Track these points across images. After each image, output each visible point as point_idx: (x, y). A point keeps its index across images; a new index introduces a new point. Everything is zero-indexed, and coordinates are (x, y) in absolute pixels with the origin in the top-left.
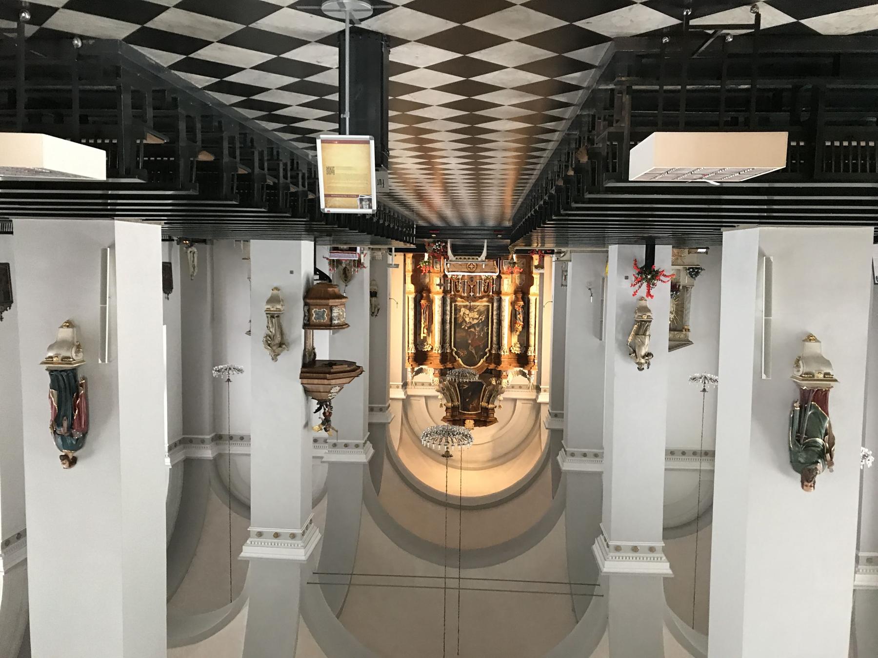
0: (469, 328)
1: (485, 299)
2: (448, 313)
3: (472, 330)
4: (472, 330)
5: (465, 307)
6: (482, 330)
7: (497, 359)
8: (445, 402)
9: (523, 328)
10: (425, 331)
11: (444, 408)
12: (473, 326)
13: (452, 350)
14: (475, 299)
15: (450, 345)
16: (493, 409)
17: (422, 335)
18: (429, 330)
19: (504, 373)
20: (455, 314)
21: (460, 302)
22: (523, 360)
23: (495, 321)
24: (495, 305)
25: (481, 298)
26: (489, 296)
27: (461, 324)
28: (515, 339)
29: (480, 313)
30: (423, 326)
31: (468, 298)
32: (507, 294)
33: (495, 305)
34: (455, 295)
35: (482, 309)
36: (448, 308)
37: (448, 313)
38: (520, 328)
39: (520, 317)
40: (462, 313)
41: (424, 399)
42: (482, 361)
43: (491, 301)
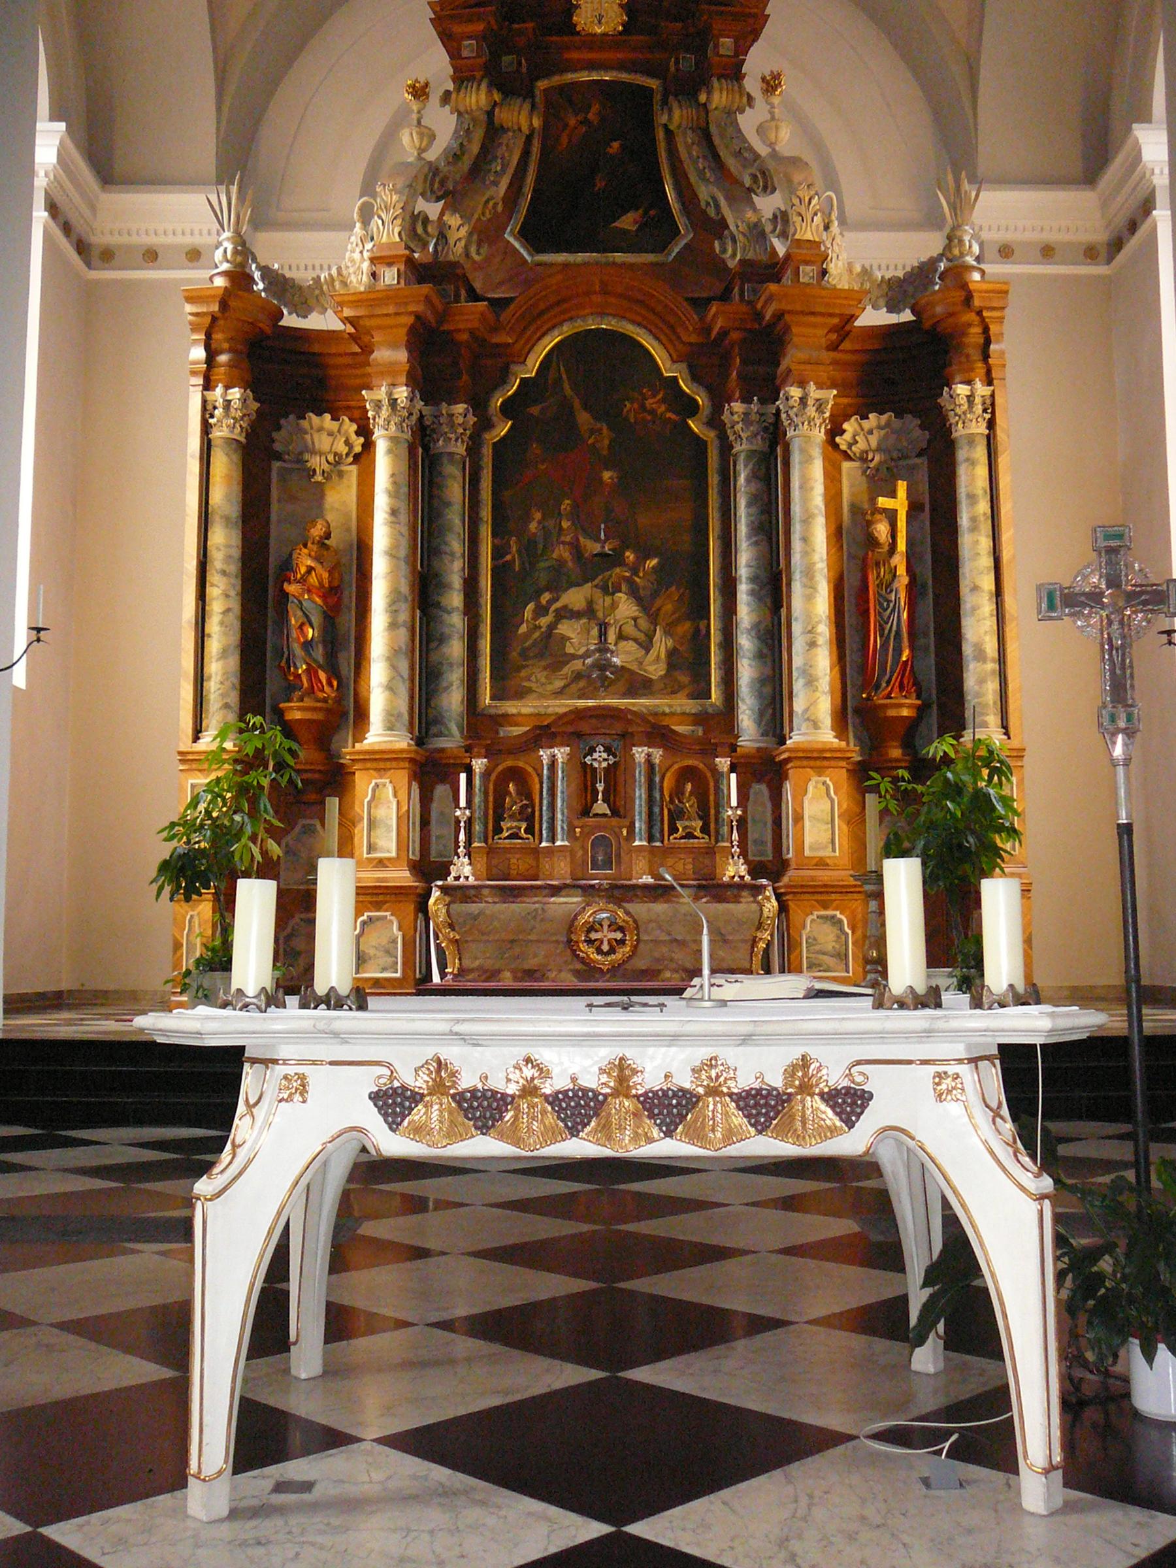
0: (612, 560)
1: (517, 731)
2: (745, 642)
3: (592, 547)
5: (637, 685)
7: (442, 363)
8: (748, 122)
9: (287, 566)
10: (882, 530)
11: (752, 84)
13: (715, 421)
14: (572, 729)
16: (462, 78)
17: (899, 503)
18: (855, 542)
19: (390, 276)
20: (700, 642)
21: (675, 706)
22: (278, 368)
23: (455, 599)
24: (453, 700)
28: (340, 499)
29: (550, 650)
30: (899, 562)
31: (623, 729)
32: (380, 760)
33: (453, 700)
35: (535, 675)
36: (746, 672)
37: (745, 642)
38: (304, 561)
39: (304, 628)
40: (662, 644)
41: (856, 200)
43: (481, 726)
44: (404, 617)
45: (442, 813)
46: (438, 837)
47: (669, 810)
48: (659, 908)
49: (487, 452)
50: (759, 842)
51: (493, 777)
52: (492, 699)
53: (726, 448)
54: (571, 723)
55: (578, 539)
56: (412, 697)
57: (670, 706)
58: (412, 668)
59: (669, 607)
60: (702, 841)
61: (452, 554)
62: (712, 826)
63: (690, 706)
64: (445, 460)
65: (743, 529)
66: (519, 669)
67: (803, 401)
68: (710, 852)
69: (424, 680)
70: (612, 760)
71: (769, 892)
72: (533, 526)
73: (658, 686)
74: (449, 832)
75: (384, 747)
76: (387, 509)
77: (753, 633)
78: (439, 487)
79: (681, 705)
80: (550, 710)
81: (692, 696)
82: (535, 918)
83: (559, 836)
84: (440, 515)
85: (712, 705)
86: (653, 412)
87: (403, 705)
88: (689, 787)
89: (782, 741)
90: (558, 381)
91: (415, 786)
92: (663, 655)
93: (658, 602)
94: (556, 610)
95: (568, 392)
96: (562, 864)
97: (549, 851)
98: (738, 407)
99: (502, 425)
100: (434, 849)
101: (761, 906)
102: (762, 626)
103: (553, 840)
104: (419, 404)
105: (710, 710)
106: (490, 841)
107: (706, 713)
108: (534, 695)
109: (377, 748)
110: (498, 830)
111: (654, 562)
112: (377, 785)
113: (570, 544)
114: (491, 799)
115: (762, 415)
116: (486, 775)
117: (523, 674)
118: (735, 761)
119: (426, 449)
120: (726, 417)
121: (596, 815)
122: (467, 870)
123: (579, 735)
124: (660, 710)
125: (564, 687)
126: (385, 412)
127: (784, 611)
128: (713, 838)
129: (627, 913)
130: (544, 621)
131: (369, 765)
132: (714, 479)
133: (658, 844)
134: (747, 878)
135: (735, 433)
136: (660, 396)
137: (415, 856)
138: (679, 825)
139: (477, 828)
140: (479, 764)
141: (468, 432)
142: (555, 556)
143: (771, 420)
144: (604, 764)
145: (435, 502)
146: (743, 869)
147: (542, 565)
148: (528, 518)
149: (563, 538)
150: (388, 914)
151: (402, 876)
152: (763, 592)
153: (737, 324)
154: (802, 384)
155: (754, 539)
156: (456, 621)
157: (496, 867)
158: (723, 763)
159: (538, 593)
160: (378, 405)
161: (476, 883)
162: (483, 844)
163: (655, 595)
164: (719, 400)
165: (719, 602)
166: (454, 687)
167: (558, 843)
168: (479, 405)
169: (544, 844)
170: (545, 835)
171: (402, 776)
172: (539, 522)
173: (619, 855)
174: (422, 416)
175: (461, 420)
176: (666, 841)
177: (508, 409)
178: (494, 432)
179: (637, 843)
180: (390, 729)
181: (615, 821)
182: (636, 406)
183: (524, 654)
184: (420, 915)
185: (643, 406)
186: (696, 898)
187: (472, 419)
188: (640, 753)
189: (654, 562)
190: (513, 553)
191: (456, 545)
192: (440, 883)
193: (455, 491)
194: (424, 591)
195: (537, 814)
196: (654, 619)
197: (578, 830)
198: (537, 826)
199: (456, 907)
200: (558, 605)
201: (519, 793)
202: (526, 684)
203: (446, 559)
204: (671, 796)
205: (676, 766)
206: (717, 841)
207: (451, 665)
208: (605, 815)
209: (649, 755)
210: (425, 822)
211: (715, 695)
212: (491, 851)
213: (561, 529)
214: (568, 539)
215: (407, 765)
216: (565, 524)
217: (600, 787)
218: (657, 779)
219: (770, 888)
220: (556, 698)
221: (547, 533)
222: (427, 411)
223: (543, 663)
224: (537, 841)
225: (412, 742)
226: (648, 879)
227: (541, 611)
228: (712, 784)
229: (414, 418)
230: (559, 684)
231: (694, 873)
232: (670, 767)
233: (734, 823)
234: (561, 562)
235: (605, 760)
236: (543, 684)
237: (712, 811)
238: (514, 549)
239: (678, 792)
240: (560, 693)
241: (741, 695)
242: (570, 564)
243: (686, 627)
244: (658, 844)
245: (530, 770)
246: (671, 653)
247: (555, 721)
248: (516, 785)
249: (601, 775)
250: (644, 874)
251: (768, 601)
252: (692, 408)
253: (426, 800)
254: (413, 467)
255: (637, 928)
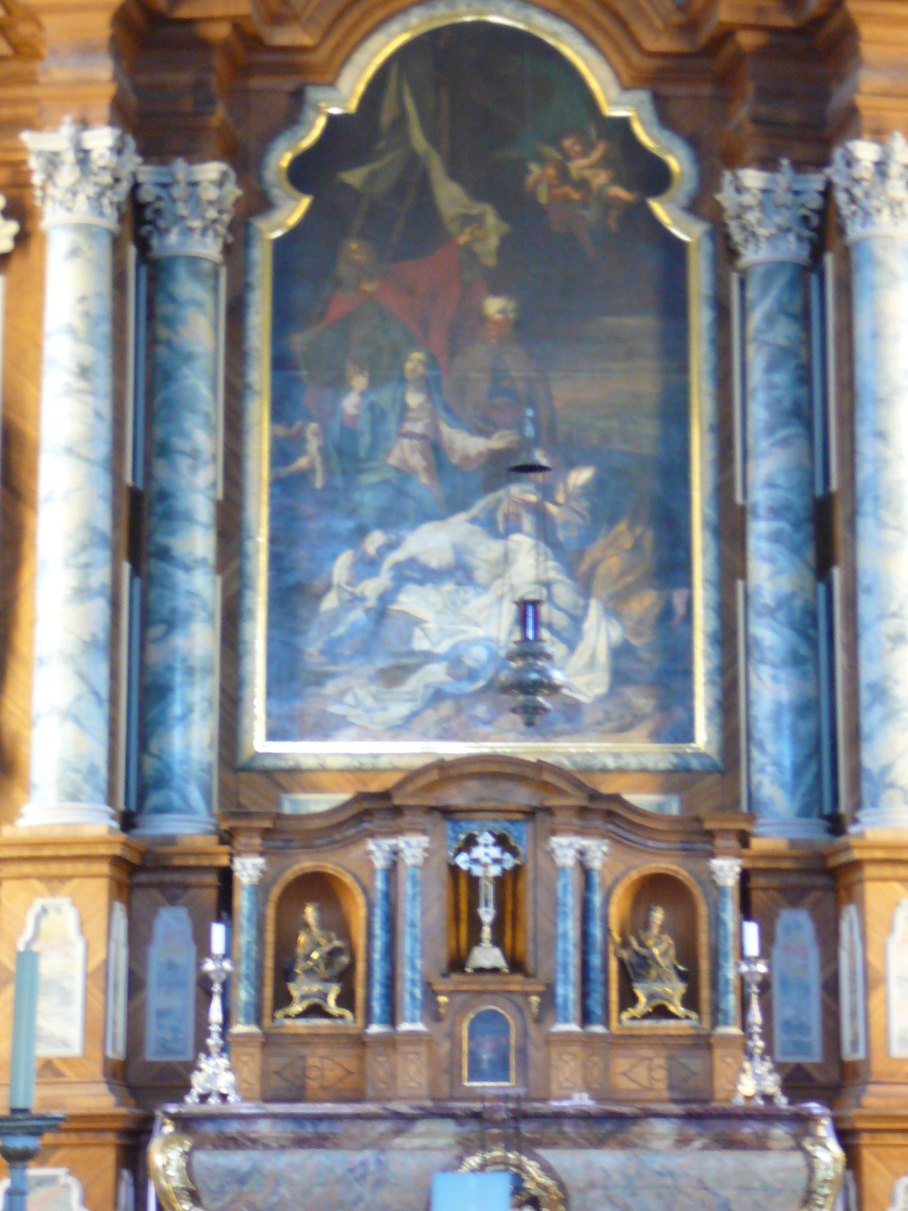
1: (318, 803)
2: (768, 635)
3: (467, 444)
4: (467, 444)
6: (347, 456)
12: (458, 487)
13: (701, 205)
15: (726, 252)
20: (672, 626)
23: (198, 542)
25: (378, 807)
26: (279, 836)
27: (603, 506)
33: (191, 740)
34: (698, 839)
37: (768, 635)
42: (346, 94)
43: (247, 792)
44: (101, 576)
45: (171, 966)
46: (161, 1014)
47: (621, 962)
48: (608, 1160)
49: (262, 260)
50: (795, 1027)
51: (276, 891)
52: (273, 735)
53: (726, 252)
54: (431, 787)
55: (437, 431)
56: (113, 734)
57: (617, 756)
58: (114, 675)
59: (613, 563)
60: (683, 1024)
61: (194, 455)
62: (705, 993)
63: (655, 754)
64: (181, 272)
65: (759, 413)
66: (320, 679)
67: (881, 167)
68: (702, 1043)
69: (139, 701)
70: (509, 861)
71: (824, 1129)
72: (351, 403)
73: (588, 718)
74: (182, 1001)
75: (58, 833)
76: (72, 365)
77: (781, 615)
78: (170, 322)
79: (636, 754)
80: (383, 763)
81: (656, 736)
82: (362, 1177)
83: (407, 1014)
84: (169, 377)
85: (698, 755)
86: (583, 185)
87: (96, 750)
88: (658, 916)
89: (836, 825)
90: (401, 120)
91: (120, 911)
92: (603, 656)
93: (593, 553)
94: (398, 567)
95: (419, 140)
96: (412, 1069)
97: (390, 1043)
98: (752, 178)
99: (292, 203)
100: (153, 1033)
101: (810, 1158)
102: (798, 603)
103: (391, 1018)
104: (132, 161)
105: (695, 764)
106: (267, 1022)
107: (688, 770)
108: (352, 732)
109: (45, 834)
110: (283, 999)
111: (581, 476)
112: (44, 910)
113: (422, 437)
114: (270, 937)
115: (796, 193)
116: (261, 889)
117: (331, 688)
118: (749, 864)
119: (143, 246)
120: (726, 197)
121: (480, 971)
122: (225, 1082)
123: (447, 812)
124: (597, 763)
125: (414, 715)
126: (67, 175)
127: (837, 574)
128: (706, 1018)
129: (547, 1169)
130: (372, 588)
131: (27, 869)
132: (700, 318)
133: (598, 1029)
134: (782, 1102)
135: (744, 228)
136: (597, 154)
137: (117, 1050)
138: (640, 992)
139: (243, 994)
140: (248, 869)
141: (226, 218)
142: (393, 460)
143: (815, 202)
144: (495, 871)
145: (162, 352)
146: (772, 1084)
147: (369, 479)
148: (340, 384)
149: (409, 427)
150: (60, 1172)
151: (98, 1098)
152: (799, 537)
153: (751, 19)
154: (879, 135)
155: (781, 433)
156: (200, 586)
157: (278, 1073)
158: (727, 870)
159: (361, 532)
160: (53, 161)
161: (247, 1108)
162: (253, 1029)
163: (589, 537)
164: (715, 159)
165: (712, 556)
166: (196, 716)
167: (404, 1027)
168: (245, 161)
169: (375, 1029)
170: (377, 1007)
171: (96, 888)
172: (363, 394)
173: (522, 1052)
174: (136, 187)
175: (211, 193)
176: (614, 1024)
177: (303, 174)
178: (277, 216)
179: (560, 1027)
180: (74, 797)
181: (517, 983)
182: (551, 171)
183: (331, 651)
184: (126, 1174)
185: (564, 175)
186: (683, 1142)
187: (233, 191)
188: (565, 848)
189: (581, 476)
190: (310, 457)
191: (201, 436)
192: (172, 1109)
193: (199, 330)
194: (138, 525)
195: (361, 967)
196: (585, 586)
197: (443, 999)
198: (360, 992)
199: (203, 1158)
200: (398, 556)
201: (324, 925)
202: (336, 709)
203: (184, 463)
204: (623, 934)
205: (634, 875)
206: (715, 1023)
207: (190, 671)
208: (495, 970)
209: (582, 853)
210: (136, 984)
211: (704, 737)
212: (270, 1042)
213: (405, 408)
214: (418, 427)
215: (104, 868)
216: (414, 399)
217: (487, 914)
218: (597, 899)
219: (826, 1122)
220: (395, 738)
221: (377, 415)
222: (148, 174)
223: (369, 670)
224: (360, 1021)
225: (115, 825)
226: (582, 1100)
227: (368, 566)
228: (703, 910)
229: (125, 187)
230: (399, 710)
231: (671, 1088)
232: (625, 873)
233: (755, 989)
234: (405, 473)
235: (496, 861)
236: (368, 711)
237: (704, 965)
238: (313, 445)
239: (637, 923)
240: (401, 728)
241: (757, 735)
242: (424, 479)
243: (646, 602)
244: (598, 1029)
245: (348, 879)
246: (620, 652)
247: (400, 785)
248: (320, 910)
249: (488, 891)
250: (573, 1088)
251: (810, 554)
252: (656, 178)
253: (138, 939)
254: (119, 282)
255: (565, 1201)
